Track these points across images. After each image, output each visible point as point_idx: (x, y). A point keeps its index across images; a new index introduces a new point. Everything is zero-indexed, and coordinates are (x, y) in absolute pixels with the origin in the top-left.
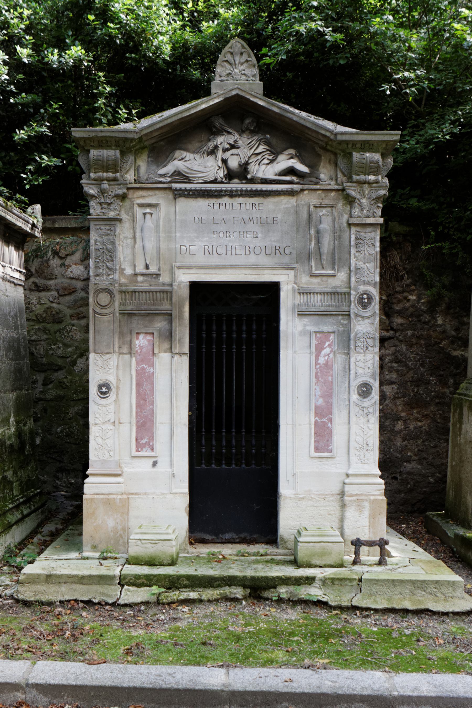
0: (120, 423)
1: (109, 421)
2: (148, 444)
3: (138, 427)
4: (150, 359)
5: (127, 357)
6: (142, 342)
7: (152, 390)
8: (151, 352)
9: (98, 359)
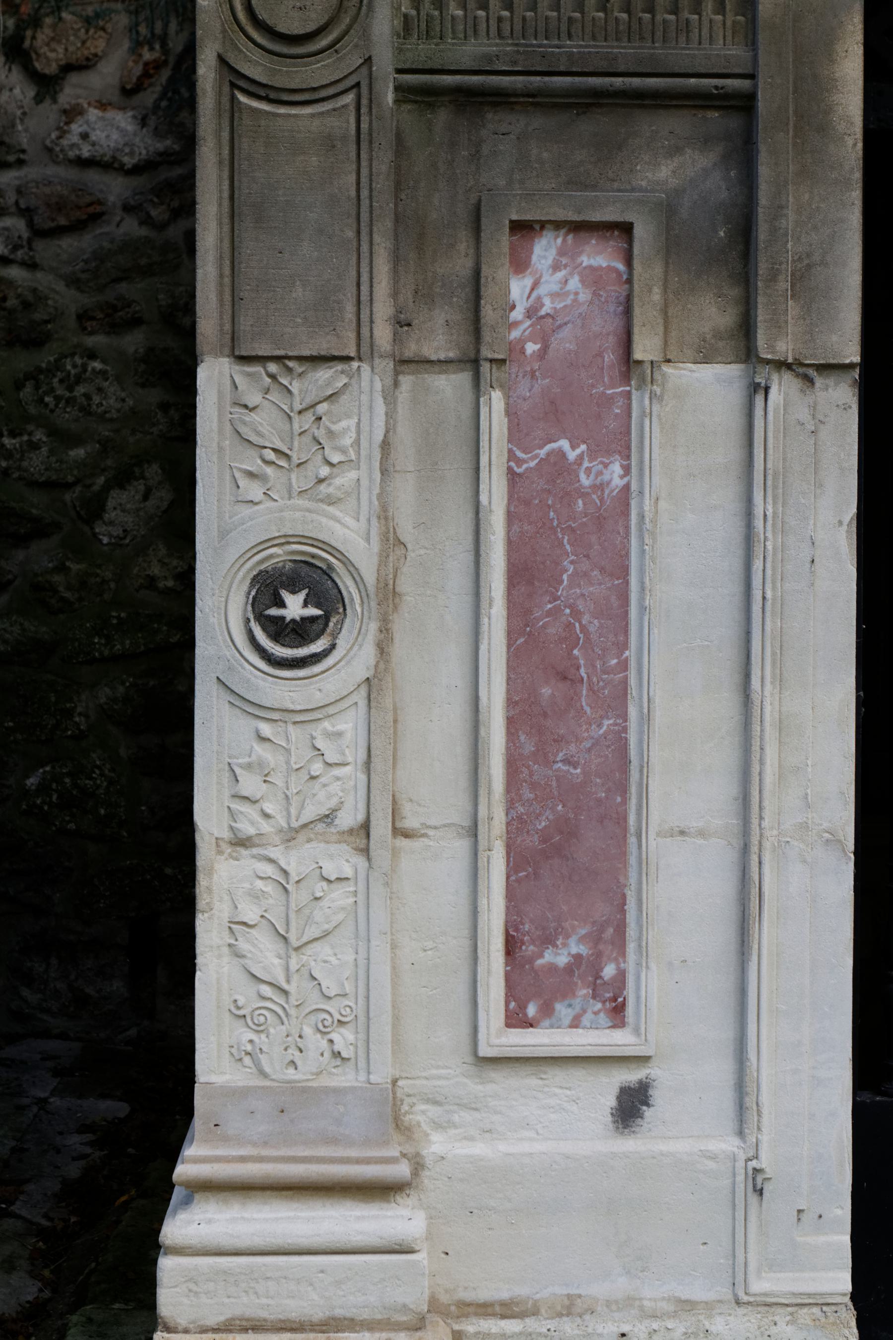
0: (399, 832)
1: (328, 818)
2: (586, 969)
3: (517, 860)
4: (611, 399)
5: (450, 386)
6: (548, 284)
7: (617, 614)
8: (610, 357)
9: (254, 399)
